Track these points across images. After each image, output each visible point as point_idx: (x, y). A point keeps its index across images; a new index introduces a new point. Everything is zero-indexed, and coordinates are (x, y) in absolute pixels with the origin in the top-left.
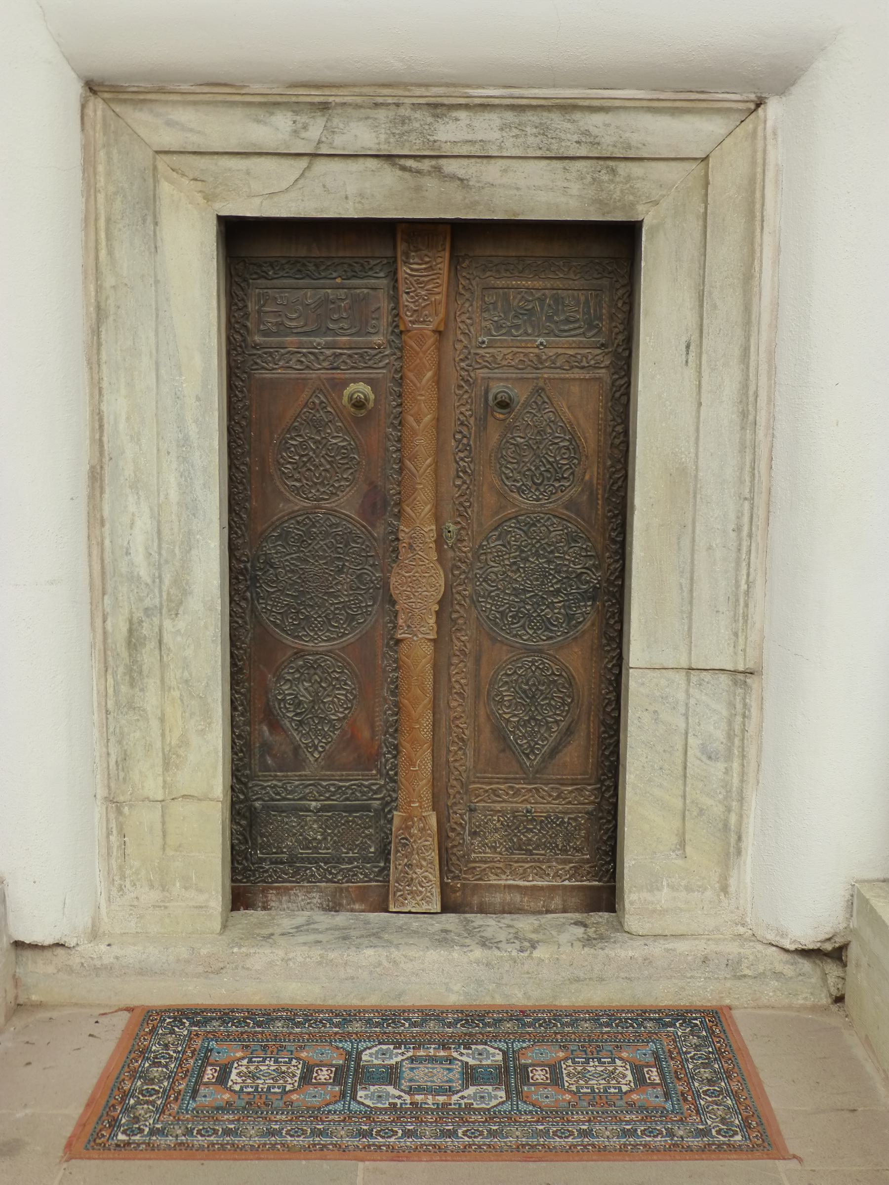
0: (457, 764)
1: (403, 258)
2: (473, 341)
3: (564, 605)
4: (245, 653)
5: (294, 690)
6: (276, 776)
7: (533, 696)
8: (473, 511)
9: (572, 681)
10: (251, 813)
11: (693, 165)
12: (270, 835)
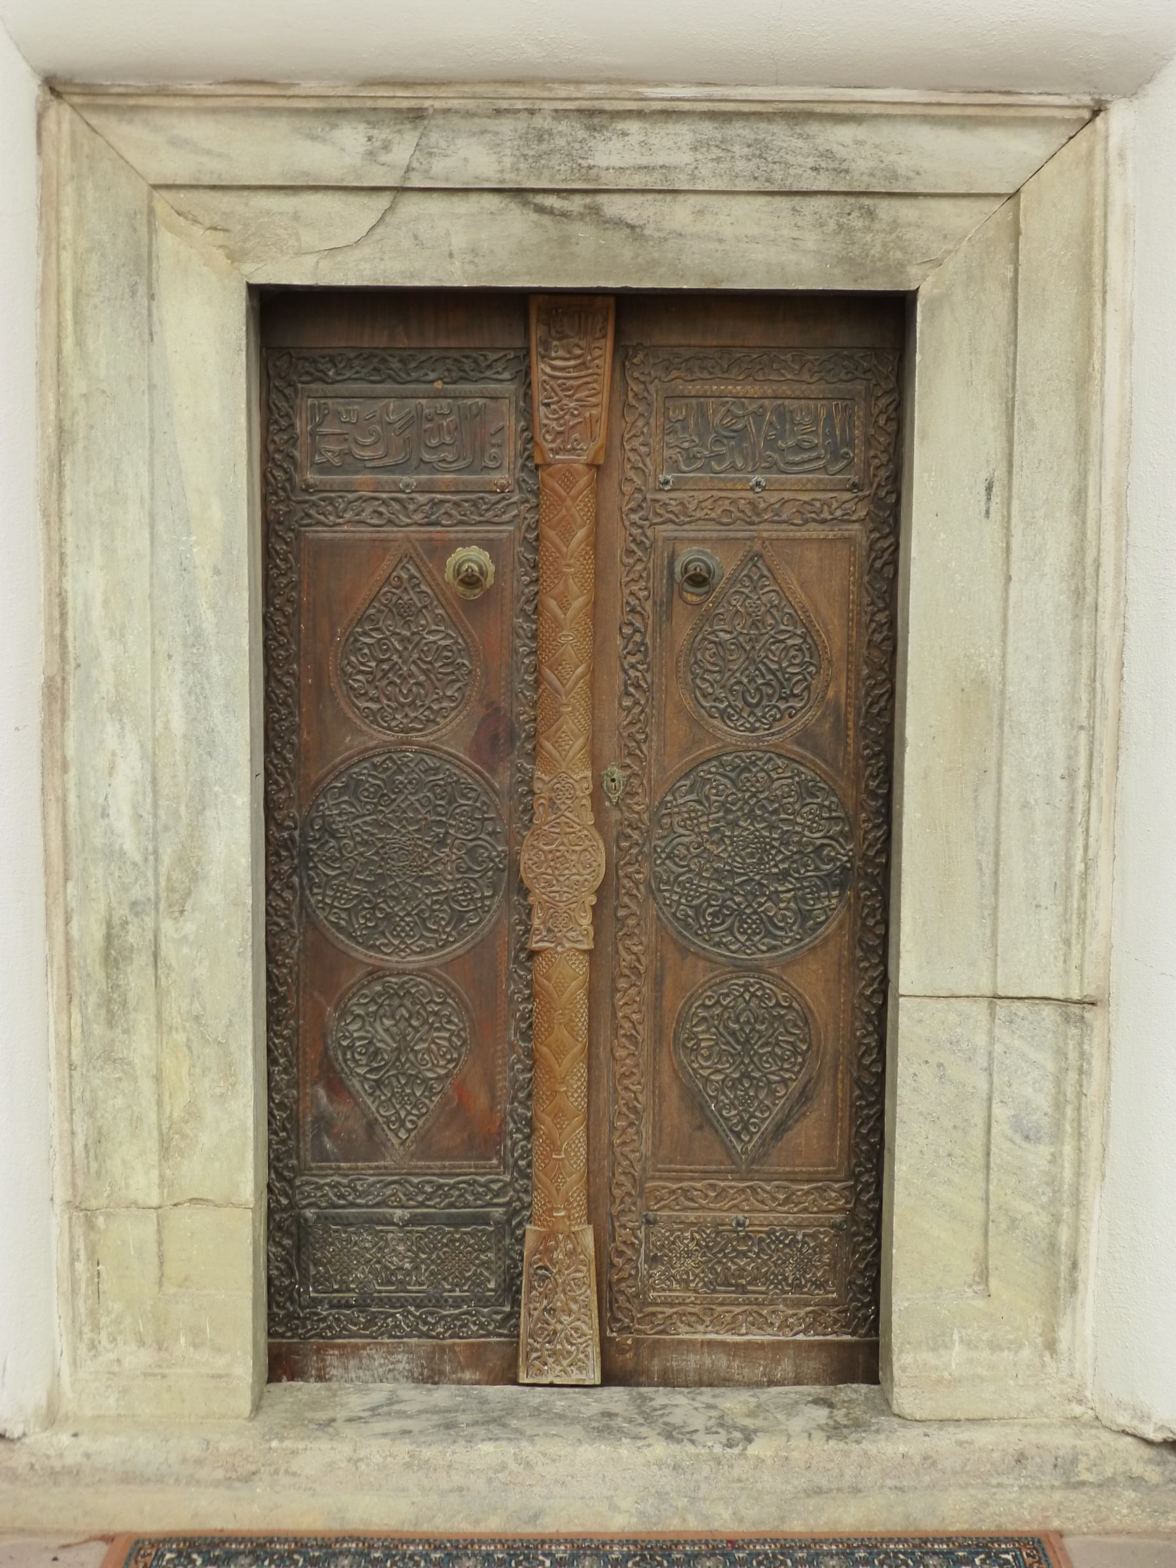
0: (626, 1149)
1: (541, 350)
2: (651, 480)
3: (794, 896)
4: (291, 972)
5: (368, 1032)
6: (339, 1168)
7: (748, 1040)
8: (650, 748)
9: (808, 1016)
10: (299, 1227)
11: (995, 205)
12: (330, 1262)
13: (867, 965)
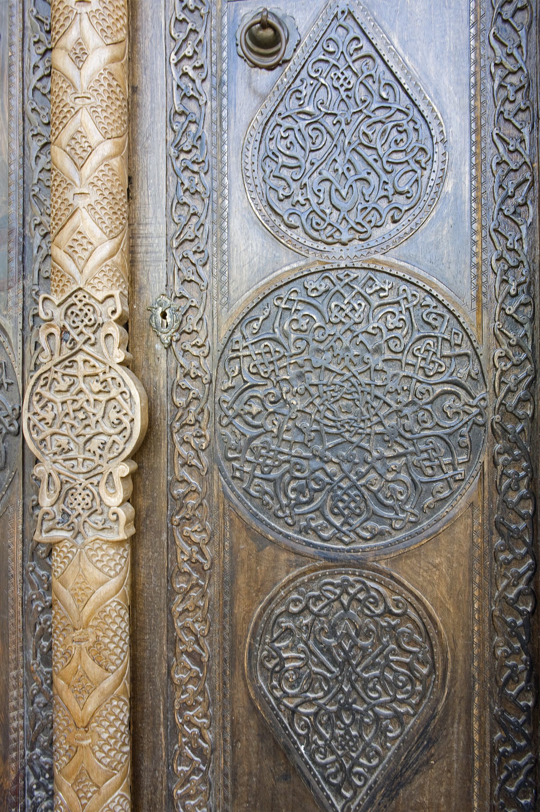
7: (347, 660)
13: (510, 557)
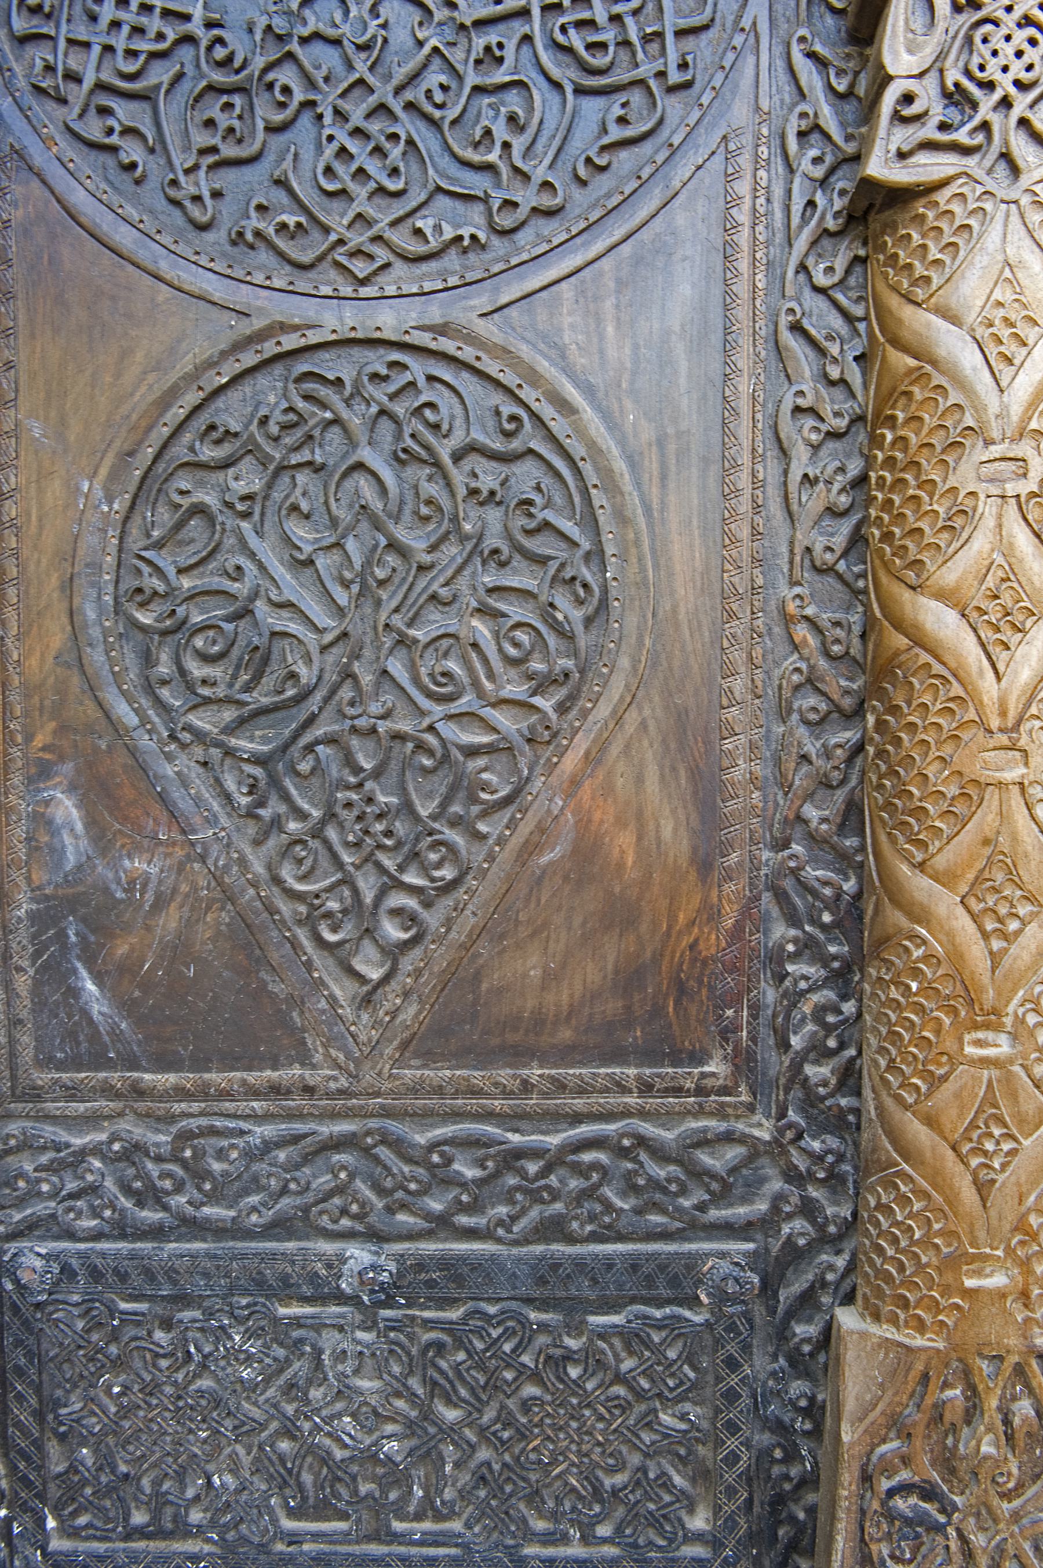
6: (139, 1092)
